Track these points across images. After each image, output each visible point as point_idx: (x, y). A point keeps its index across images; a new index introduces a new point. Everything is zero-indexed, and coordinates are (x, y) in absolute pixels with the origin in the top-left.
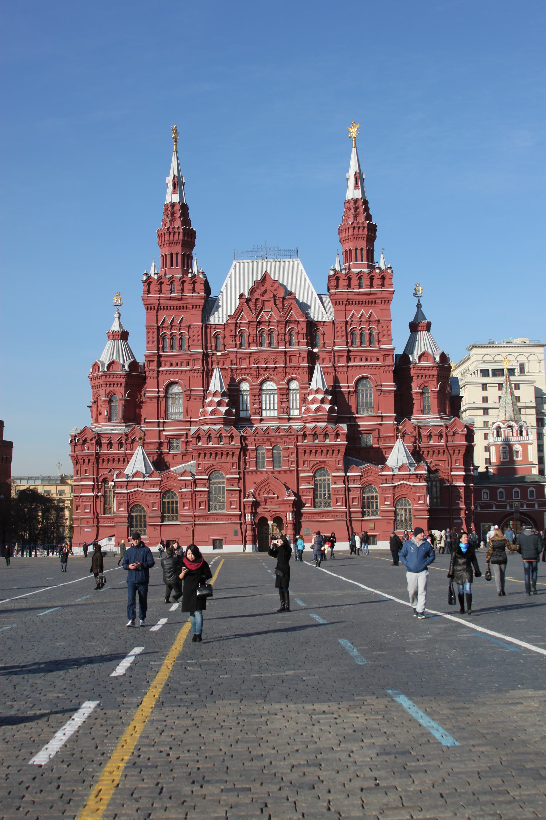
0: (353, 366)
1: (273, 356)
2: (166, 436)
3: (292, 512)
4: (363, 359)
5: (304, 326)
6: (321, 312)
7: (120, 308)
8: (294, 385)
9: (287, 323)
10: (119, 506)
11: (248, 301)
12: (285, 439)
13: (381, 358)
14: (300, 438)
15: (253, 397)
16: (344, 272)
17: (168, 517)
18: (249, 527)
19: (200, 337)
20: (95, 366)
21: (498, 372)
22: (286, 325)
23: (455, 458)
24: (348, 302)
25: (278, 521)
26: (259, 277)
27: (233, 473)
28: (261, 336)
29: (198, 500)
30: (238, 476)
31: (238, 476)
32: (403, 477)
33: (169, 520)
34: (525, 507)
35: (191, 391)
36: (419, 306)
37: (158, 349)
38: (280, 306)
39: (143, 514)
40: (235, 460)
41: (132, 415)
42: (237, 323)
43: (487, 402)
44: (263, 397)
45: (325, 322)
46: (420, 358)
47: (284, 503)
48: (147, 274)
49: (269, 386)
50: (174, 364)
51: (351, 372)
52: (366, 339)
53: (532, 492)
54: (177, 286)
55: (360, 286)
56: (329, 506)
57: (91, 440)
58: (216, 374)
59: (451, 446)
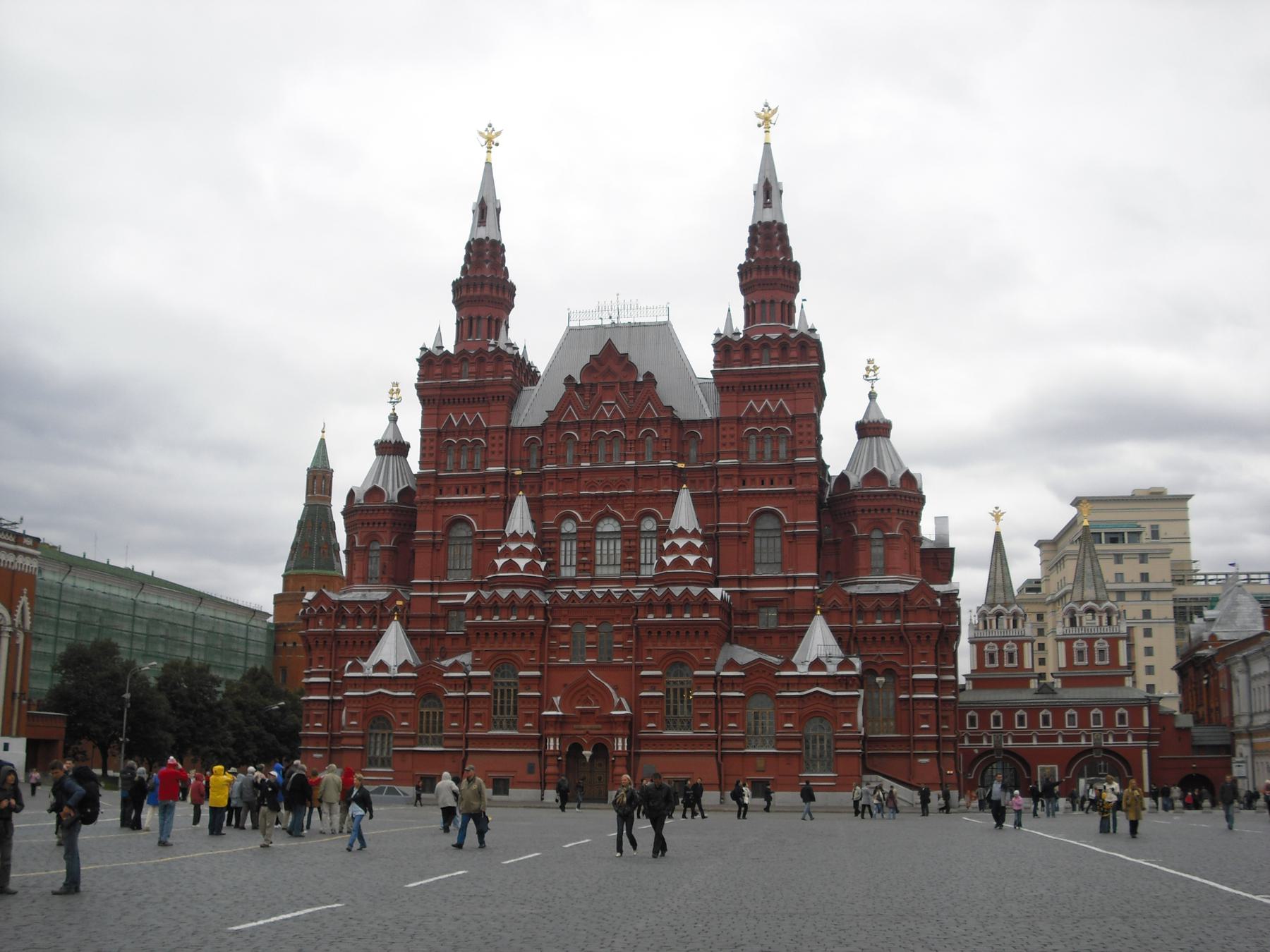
2: (443, 605)
4: (767, 481)
7: (397, 406)
9: (640, 423)
10: (351, 716)
12: (618, 612)
14: (641, 611)
15: (582, 545)
16: (736, 338)
17: (427, 738)
19: (503, 449)
22: (638, 425)
25: (601, 750)
30: (538, 673)
31: (538, 673)
33: (427, 744)
35: (484, 534)
36: (872, 396)
39: (386, 732)
40: (534, 647)
42: (559, 424)
44: (598, 546)
45: (704, 420)
47: (612, 720)
48: (423, 349)
49: (608, 526)
50: (461, 490)
53: (1122, 717)
57: (330, 610)
58: (520, 507)
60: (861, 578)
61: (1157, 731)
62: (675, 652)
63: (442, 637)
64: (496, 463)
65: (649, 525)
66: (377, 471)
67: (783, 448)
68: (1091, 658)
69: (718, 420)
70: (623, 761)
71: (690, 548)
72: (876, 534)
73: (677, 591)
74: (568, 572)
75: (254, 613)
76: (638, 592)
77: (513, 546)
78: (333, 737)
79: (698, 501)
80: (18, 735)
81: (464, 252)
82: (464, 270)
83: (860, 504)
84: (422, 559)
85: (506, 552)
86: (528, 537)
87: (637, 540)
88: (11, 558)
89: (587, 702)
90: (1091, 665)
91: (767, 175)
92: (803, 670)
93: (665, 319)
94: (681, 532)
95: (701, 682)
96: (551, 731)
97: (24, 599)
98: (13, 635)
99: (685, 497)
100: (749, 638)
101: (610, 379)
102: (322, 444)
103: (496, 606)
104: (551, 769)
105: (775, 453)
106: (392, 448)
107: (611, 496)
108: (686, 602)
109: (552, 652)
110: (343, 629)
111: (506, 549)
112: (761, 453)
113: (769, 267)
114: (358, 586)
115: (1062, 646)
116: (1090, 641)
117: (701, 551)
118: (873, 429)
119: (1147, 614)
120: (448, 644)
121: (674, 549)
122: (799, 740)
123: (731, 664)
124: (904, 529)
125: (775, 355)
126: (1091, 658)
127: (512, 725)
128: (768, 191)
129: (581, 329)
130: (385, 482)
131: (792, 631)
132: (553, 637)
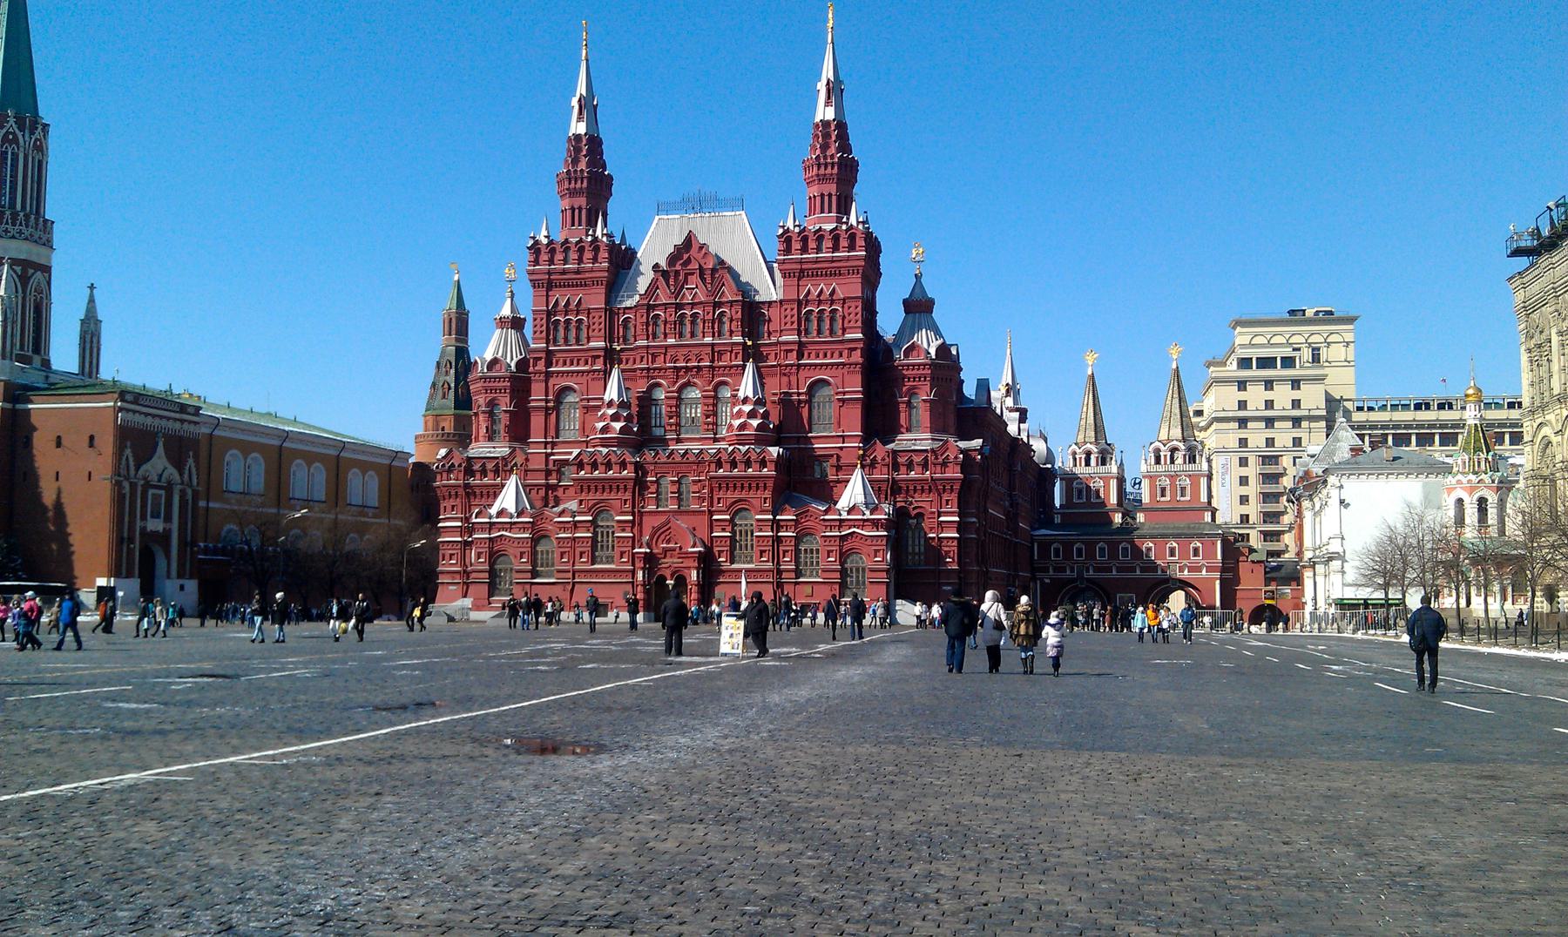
0: (806, 365)
1: (696, 351)
3: (698, 569)
5: (739, 308)
6: (768, 289)
8: (726, 393)
9: (717, 305)
10: (479, 555)
11: (665, 274)
13: (845, 353)
18: (640, 588)
21: (1267, 363)
23: (945, 497)
24: (802, 274)
25: (681, 581)
26: (679, 241)
27: (623, 513)
28: (682, 324)
32: (854, 523)
37: (548, 343)
38: (709, 280)
40: (628, 496)
43: (1245, 408)
45: (770, 303)
46: (907, 354)
47: (687, 556)
49: (694, 393)
51: (802, 374)
52: (826, 325)
54: (573, 255)
55: (819, 250)
56: (751, 562)
62: (741, 500)
63: (554, 488)
64: (597, 338)
68: (1173, 495)
73: (743, 449)
74: (658, 432)
76: (712, 448)
80: (191, 578)
84: (537, 421)
87: (715, 405)
88: (177, 425)
94: (745, 400)
97: (191, 461)
98: (183, 492)
99: (750, 367)
116: (1173, 478)
117: (765, 416)
118: (918, 307)
119: (1297, 442)
120: (560, 493)
127: (610, 560)
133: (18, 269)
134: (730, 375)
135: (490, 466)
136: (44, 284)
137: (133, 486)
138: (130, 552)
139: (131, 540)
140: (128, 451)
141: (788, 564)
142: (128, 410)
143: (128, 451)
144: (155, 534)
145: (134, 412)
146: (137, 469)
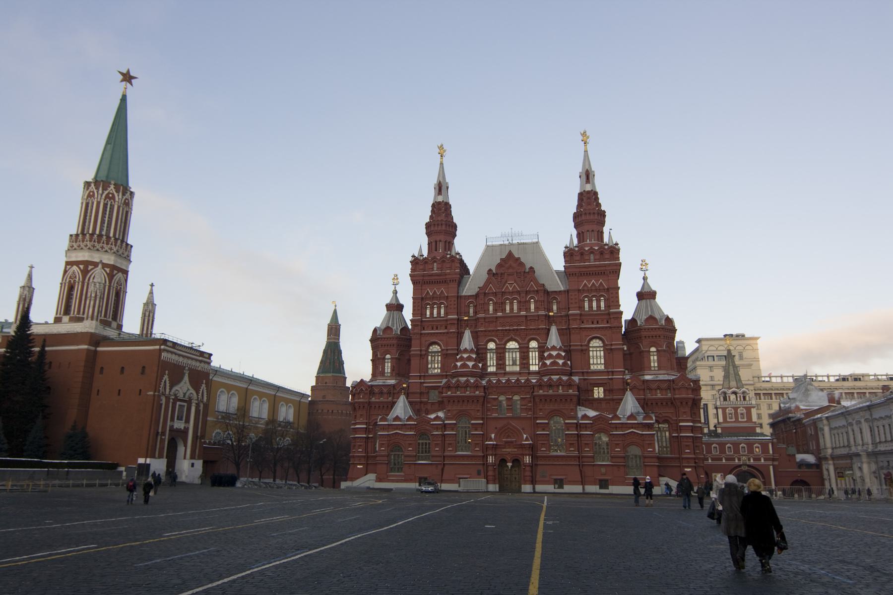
4: (595, 322)
5: (541, 294)
9: (527, 293)
10: (381, 445)
14: (536, 388)
20: (375, 330)
25: (516, 462)
27: (476, 419)
28: (505, 303)
29: (447, 442)
32: (632, 426)
34: (752, 461)
36: (645, 279)
41: (402, 369)
42: (485, 293)
44: (507, 354)
47: (522, 446)
48: (413, 256)
49: (512, 345)
59: (678, 399)
60: (646, 372)
61: (777, 456)
63: (426, 403)
64: (452, 314)
65: (533, 344)
66: (387, 319)
67: (602, 304)
69: (567, 292)
70: (528, 469)
71: (559, 356)
72: (653, 349)
74: (492, 369)
75: (303, 395)
77: (465, 356)
78: (368, 457)
79: (561, 332)
80: (199, 459)
81: (431, 209)
82: (431, 217)
83: (644, 334)
84: (415, 362)
85: (462, 359)
86: (472, 351)
88: (198, 364)
89: (508, 437)
90: (737, 421)
91: (587, 167)
92: (623, 421)
93: (535, 240)
94: (554, 348)
95: (568, 426)
96: (490, 452)
97: (204, 385)
98: (198, 405)
100: (592, 403)
101: (511, 271)
102: (335, 312)
103: (458, 386)
104: (490, 473)
105: (599, 306)
106: (395, 307)
107: (514, 330)
108: (560, 383)
109: (488, 410)
110: (373, 399)
111: (462, 357)
112: (591, 307)
113: (589, 213)
114: (379, 378)
115: (720, 411)
116: (736, 409)
118: (646, 295)
120: (429, 407)
121: (550, 356)
122: (624, 457)
123: (585, 417)
124: (667, 347)
125: (597, 257)
126: (737, 418)
128: (588, 176)
129: (493, 246)
130: (393, 324)
131: (613, 400)
132: (488, 402)
133: (108, 270)
134: (538, 335)
135: (385, 390)
136: (123, 280)
137: (168, 399)
138: (162, 441)
139: (163, 433)
140: (166, 377)
141: (587, 451)
142: (168, 351)
143: (166, 377)
144: (178, 431)
145: (172, 353)
146: (170, 389)
